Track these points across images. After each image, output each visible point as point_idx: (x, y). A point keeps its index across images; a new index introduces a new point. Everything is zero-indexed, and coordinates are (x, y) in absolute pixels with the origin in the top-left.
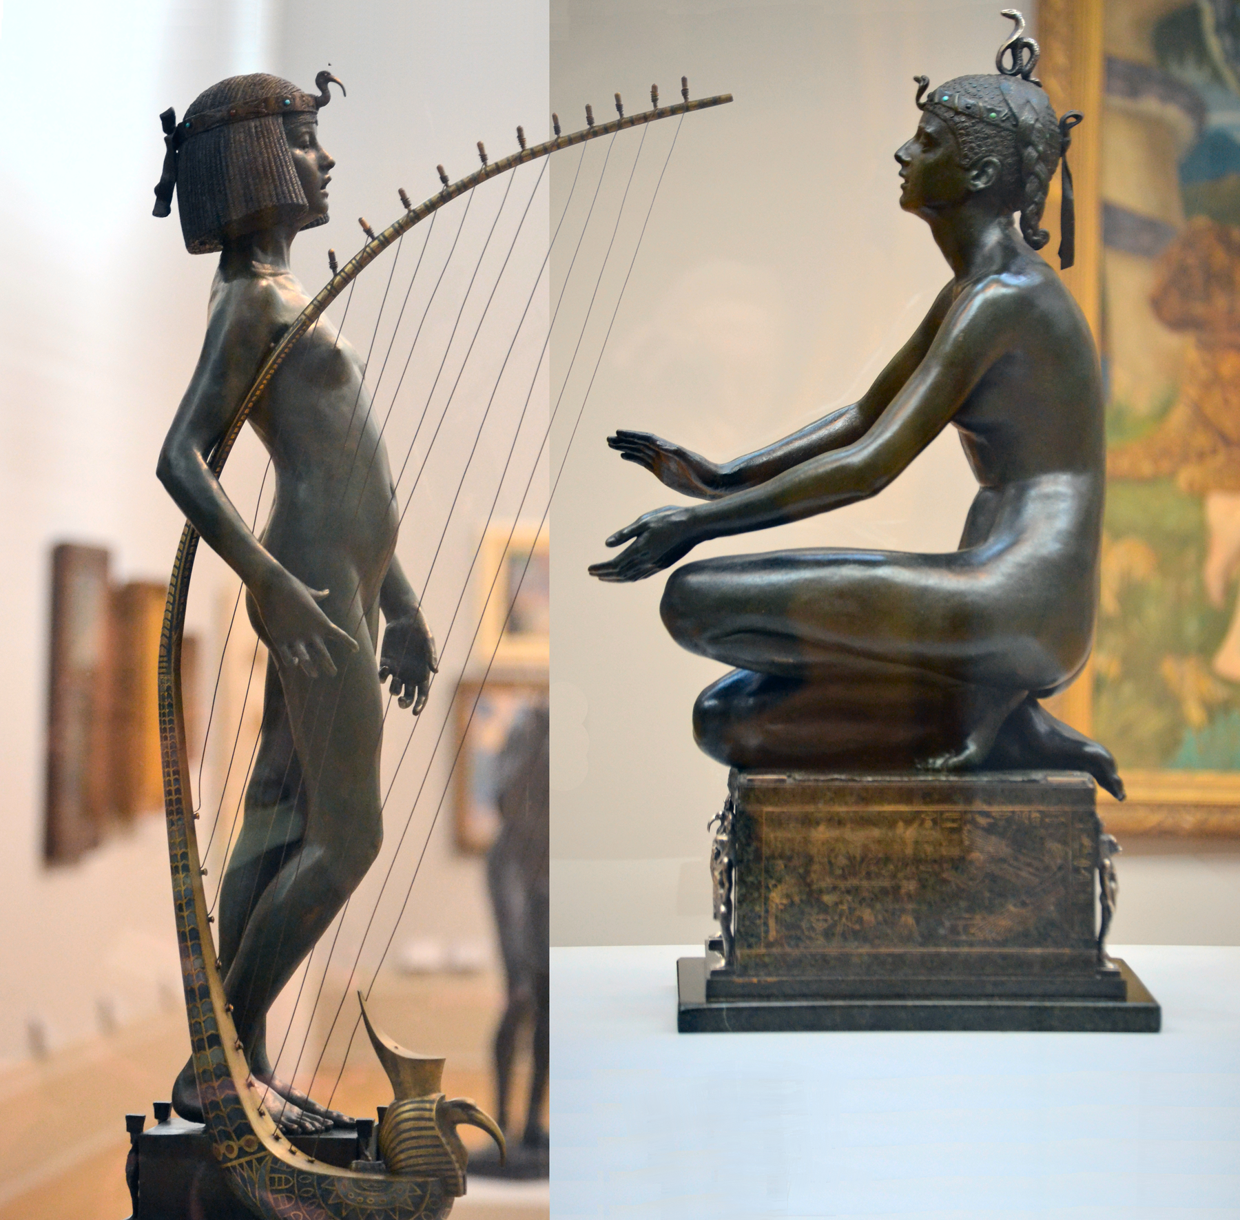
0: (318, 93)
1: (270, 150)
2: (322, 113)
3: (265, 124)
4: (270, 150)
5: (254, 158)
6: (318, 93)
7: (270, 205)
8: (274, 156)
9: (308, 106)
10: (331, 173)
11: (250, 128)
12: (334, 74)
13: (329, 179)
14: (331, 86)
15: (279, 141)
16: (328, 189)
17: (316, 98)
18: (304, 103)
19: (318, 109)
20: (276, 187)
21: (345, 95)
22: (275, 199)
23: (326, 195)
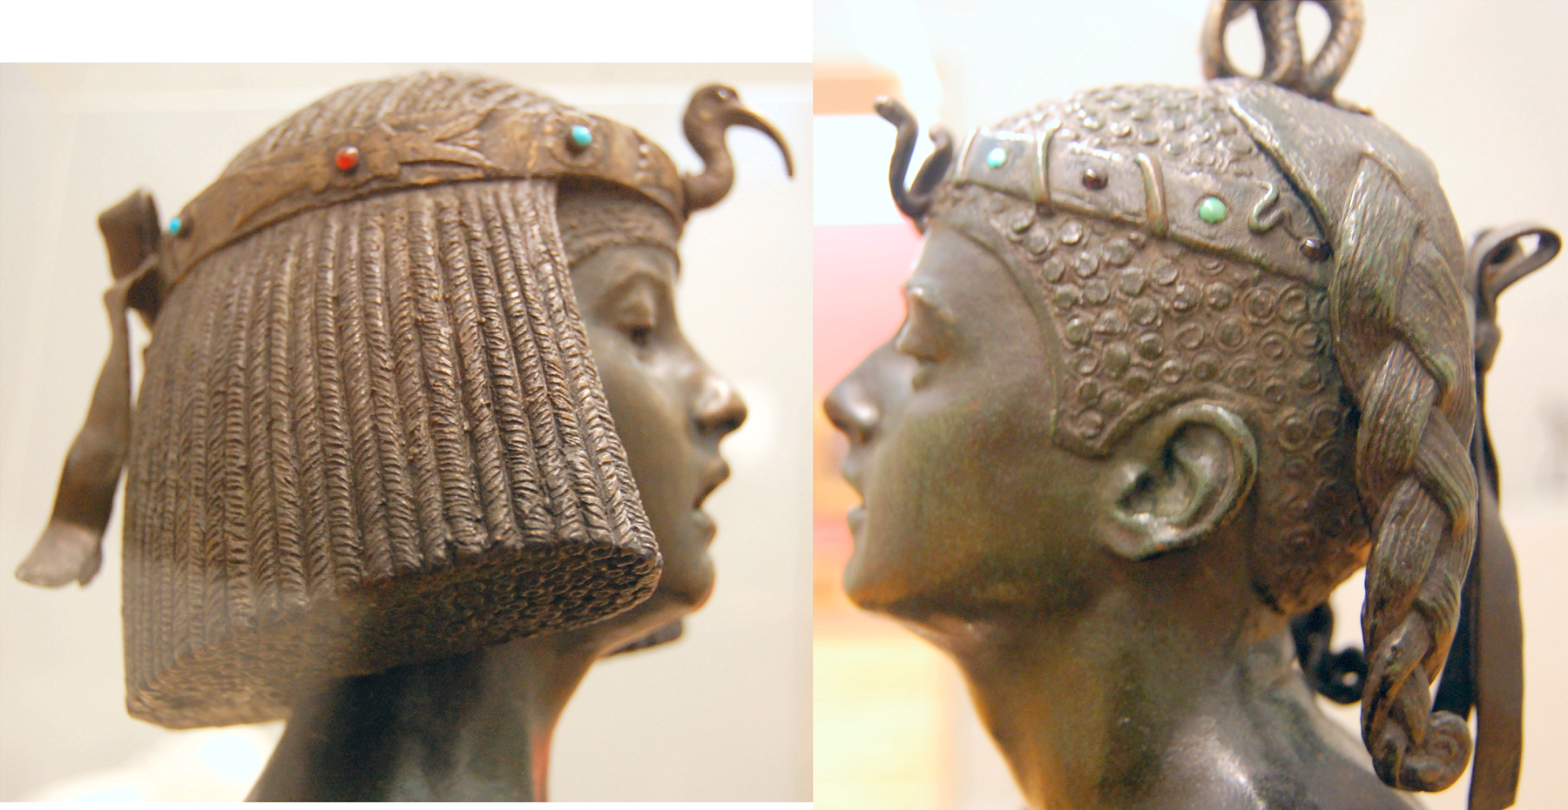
0: (687, 162)
1: (491, 296)
2: (700, 224)
3: (481, 204)
4: (491, 296)
5: (418, 325)
6: (687, 162)
7: (476, 539)
8: (509, 317)
9: (660, 186)
10: (733, 446)
11: (413, 217)
12: (751, 102)
13: (724, 473)
14: (739, 140)
15: (535, 268)
16: (714, 506)
17: (685, 183)
18: (643, 164)
19: (686, 215)
20: (510, 455)
21: (790, 171)
22: (502, 515)
23: (708, 531)
